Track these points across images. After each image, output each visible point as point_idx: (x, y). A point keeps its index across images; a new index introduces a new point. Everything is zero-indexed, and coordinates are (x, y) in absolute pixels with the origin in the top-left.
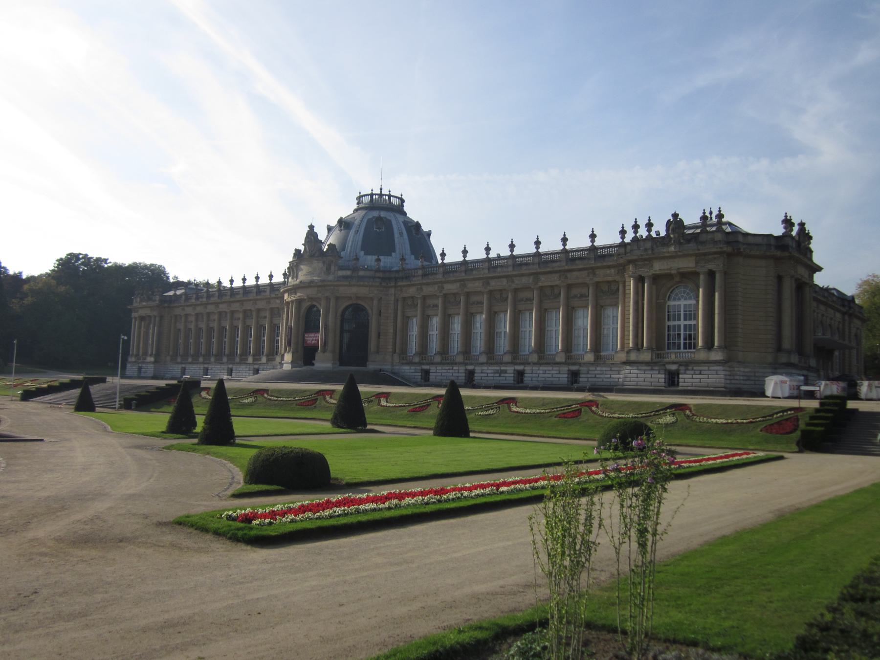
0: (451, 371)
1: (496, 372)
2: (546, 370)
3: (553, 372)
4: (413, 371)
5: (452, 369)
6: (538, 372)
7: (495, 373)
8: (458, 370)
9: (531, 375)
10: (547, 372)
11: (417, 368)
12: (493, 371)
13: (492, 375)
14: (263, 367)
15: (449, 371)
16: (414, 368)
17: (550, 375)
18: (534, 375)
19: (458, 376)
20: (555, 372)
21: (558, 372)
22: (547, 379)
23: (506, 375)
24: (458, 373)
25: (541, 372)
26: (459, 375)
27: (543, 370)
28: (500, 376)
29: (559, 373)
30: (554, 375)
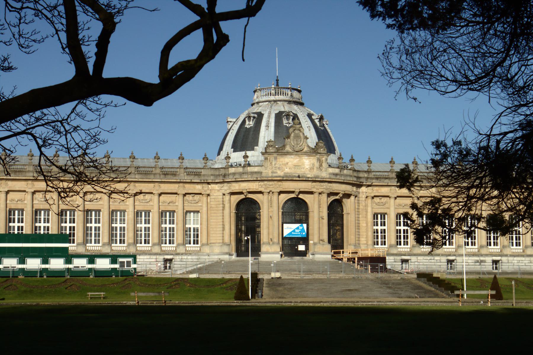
0: (433, 261)
1: (477, 261)
2: (519, 260)
3: (525, 262)
4: (393, 261)
5: (434, 259)
6: (513, 262)
7: (475, 262)
8: (440, 260)
9: (507, 264)
10: (520, 262)
11: (395, 258)
12: (473, 261)
13: (473, 264)
14: (180, 257)
15: (430, 261)
16: (393, 258)
17: (524, 264)
18: (510, 264)
19: (440, 265)
20: (527, 262)
21: (529, 262)
22: (521, 267)
23: (486, 264)
24: (441, 262)
25: (516, 262)
26: (441, 264)
27: (517, 260)
28: (480, 265)
29: (531, 263)
30: (527, 264)
